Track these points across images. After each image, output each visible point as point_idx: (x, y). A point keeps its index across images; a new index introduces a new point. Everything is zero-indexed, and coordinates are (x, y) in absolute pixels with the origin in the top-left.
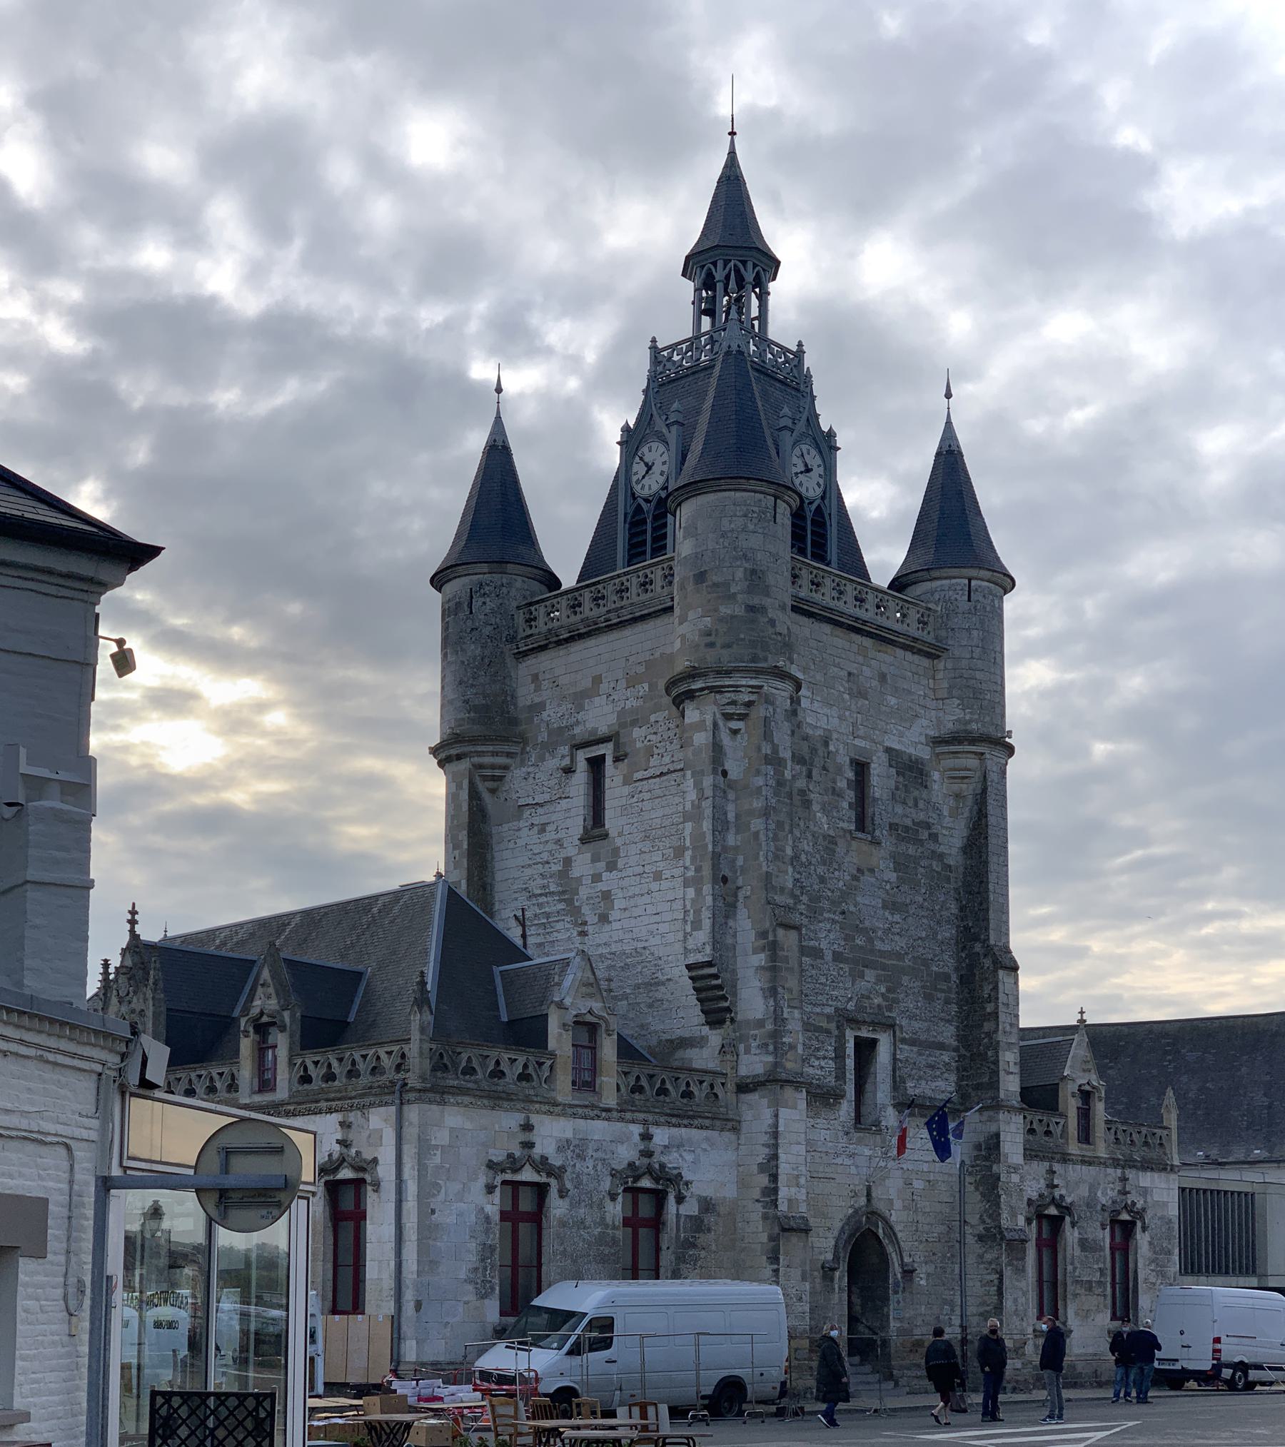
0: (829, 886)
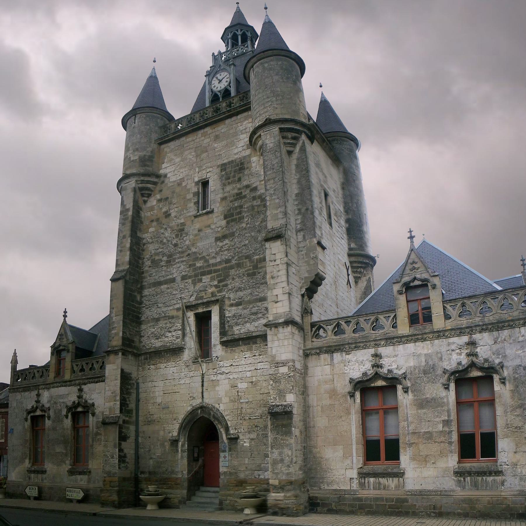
0: (180, 246)
